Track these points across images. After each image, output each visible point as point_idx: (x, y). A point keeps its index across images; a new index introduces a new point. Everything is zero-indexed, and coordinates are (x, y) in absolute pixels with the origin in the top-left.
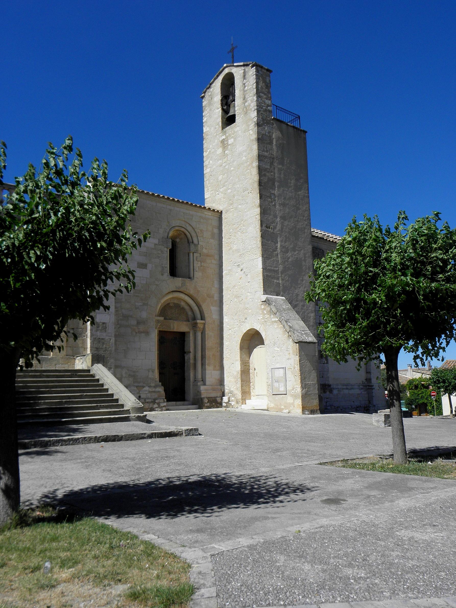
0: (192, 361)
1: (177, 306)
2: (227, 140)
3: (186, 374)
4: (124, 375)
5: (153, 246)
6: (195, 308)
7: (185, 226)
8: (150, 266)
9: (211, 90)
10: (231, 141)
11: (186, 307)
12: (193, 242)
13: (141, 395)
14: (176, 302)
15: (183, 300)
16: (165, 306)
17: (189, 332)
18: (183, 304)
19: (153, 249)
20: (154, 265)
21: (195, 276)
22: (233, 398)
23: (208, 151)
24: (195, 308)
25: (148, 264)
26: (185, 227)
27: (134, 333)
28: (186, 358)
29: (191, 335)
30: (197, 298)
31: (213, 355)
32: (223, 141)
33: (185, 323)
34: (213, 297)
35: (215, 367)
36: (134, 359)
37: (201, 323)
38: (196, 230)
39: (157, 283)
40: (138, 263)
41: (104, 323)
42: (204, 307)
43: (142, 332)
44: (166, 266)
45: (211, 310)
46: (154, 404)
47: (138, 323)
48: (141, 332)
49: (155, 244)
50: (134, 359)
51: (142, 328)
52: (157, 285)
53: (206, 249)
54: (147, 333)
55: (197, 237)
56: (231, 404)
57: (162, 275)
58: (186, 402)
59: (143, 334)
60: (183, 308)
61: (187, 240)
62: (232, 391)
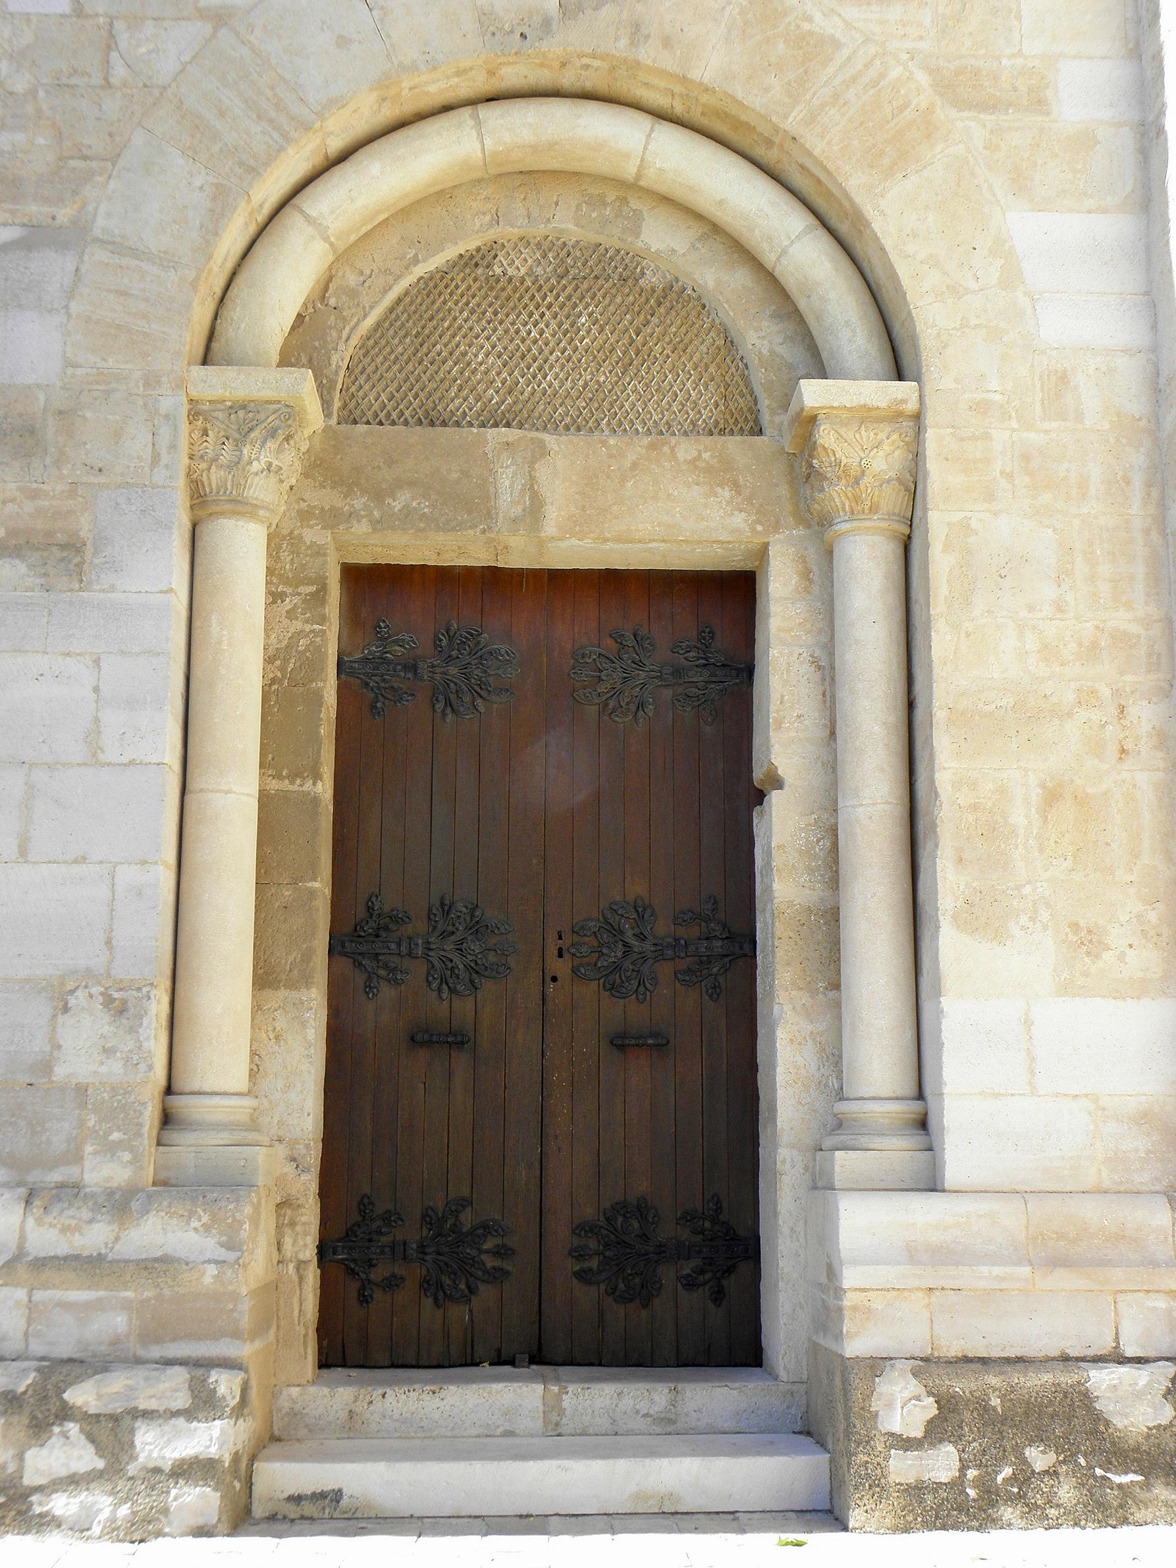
1: (599, 278)
6: (808, 259)
11: (717, 280)
15: (667, 201)
18: (661, 240)
24: (808, 259)
30: (791, 123)
31: (1052, 796)
34: (1038, 102)
35: (1087, 940)
37: (865, 416)
42: (897, 221)
46: (39, 1429)
54: (61, 554)
58: (712, 1396)
60: (675, 297)
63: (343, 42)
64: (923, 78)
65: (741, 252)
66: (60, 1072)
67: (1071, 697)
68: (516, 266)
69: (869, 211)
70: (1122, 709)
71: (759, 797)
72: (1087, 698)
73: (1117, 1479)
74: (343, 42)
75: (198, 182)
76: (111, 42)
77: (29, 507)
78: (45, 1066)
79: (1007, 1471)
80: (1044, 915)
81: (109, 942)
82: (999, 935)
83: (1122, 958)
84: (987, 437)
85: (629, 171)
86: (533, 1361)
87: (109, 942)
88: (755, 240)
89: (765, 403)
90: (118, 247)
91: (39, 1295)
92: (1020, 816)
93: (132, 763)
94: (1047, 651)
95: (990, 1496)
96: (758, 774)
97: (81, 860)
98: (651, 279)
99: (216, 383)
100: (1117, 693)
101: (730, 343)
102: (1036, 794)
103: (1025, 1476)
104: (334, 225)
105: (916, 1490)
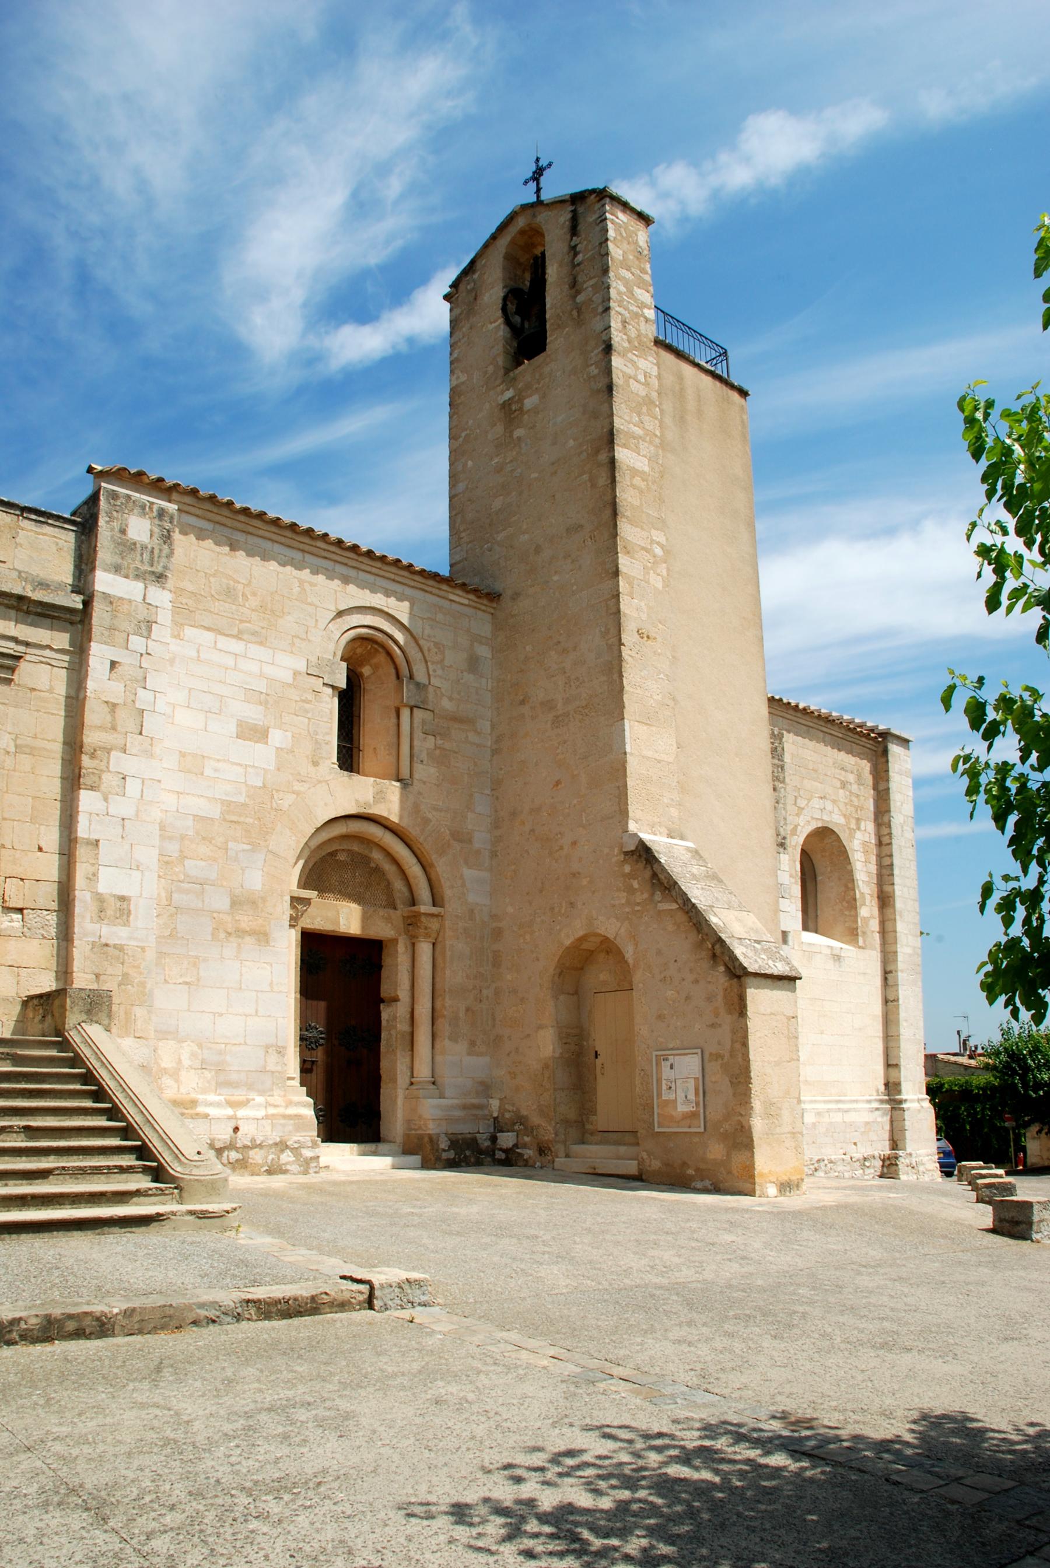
0: (403, 1027)
1: (363, 861)
2: (521, 401)
3: (384, 1064)
4: (186, 1062)
8: (277, 737)
9: (476, 276)
10: (529, 403)
11: (388, 867)
12: (411, 677)
14: (356, 847)
16: (323, 860)
17: (394, 941)
18: (376, 855)
19: (289, 685)
20: (289, 734)
21: (416, 776)
22: (527, 1139)
23: (463, 435)
25: (270, 730)
27: (222, 935)
28: (384, 1016)
29: (402, 947)
30: (421, 840)
31: (468, 1010)
32: (506, 406)
33: (382, 912)
35: (473, 1043)
36: (221, 1015)
39: (297, 787)
40: (240, 724)
41: (123, 899)
42: (442, 867)
44: (327, 738)
45: (462, 877)
46: (282, 1151)
47: (236, 903)
48: (241, 933)
49: (296, 674)
50: (221, 1015)
54: (262, 937)
56: (521, 1155)
58: (382, 1147)
59: (249, 940)
60: (378, 870)
61: (393, 671)
62: (526, 1118)
65: (395, 861)
68: (342, 857)
72: (475, 987)
74: (326, 804)
76: (273, 797)
82: (456, 1042)
85: (376, 840)
88: (401, 862)
92: (462, 1015)
94: (468, 977)
95: (461, 1161)
98: (373, 865)
101: (389, 884)
105: (448, 1160)
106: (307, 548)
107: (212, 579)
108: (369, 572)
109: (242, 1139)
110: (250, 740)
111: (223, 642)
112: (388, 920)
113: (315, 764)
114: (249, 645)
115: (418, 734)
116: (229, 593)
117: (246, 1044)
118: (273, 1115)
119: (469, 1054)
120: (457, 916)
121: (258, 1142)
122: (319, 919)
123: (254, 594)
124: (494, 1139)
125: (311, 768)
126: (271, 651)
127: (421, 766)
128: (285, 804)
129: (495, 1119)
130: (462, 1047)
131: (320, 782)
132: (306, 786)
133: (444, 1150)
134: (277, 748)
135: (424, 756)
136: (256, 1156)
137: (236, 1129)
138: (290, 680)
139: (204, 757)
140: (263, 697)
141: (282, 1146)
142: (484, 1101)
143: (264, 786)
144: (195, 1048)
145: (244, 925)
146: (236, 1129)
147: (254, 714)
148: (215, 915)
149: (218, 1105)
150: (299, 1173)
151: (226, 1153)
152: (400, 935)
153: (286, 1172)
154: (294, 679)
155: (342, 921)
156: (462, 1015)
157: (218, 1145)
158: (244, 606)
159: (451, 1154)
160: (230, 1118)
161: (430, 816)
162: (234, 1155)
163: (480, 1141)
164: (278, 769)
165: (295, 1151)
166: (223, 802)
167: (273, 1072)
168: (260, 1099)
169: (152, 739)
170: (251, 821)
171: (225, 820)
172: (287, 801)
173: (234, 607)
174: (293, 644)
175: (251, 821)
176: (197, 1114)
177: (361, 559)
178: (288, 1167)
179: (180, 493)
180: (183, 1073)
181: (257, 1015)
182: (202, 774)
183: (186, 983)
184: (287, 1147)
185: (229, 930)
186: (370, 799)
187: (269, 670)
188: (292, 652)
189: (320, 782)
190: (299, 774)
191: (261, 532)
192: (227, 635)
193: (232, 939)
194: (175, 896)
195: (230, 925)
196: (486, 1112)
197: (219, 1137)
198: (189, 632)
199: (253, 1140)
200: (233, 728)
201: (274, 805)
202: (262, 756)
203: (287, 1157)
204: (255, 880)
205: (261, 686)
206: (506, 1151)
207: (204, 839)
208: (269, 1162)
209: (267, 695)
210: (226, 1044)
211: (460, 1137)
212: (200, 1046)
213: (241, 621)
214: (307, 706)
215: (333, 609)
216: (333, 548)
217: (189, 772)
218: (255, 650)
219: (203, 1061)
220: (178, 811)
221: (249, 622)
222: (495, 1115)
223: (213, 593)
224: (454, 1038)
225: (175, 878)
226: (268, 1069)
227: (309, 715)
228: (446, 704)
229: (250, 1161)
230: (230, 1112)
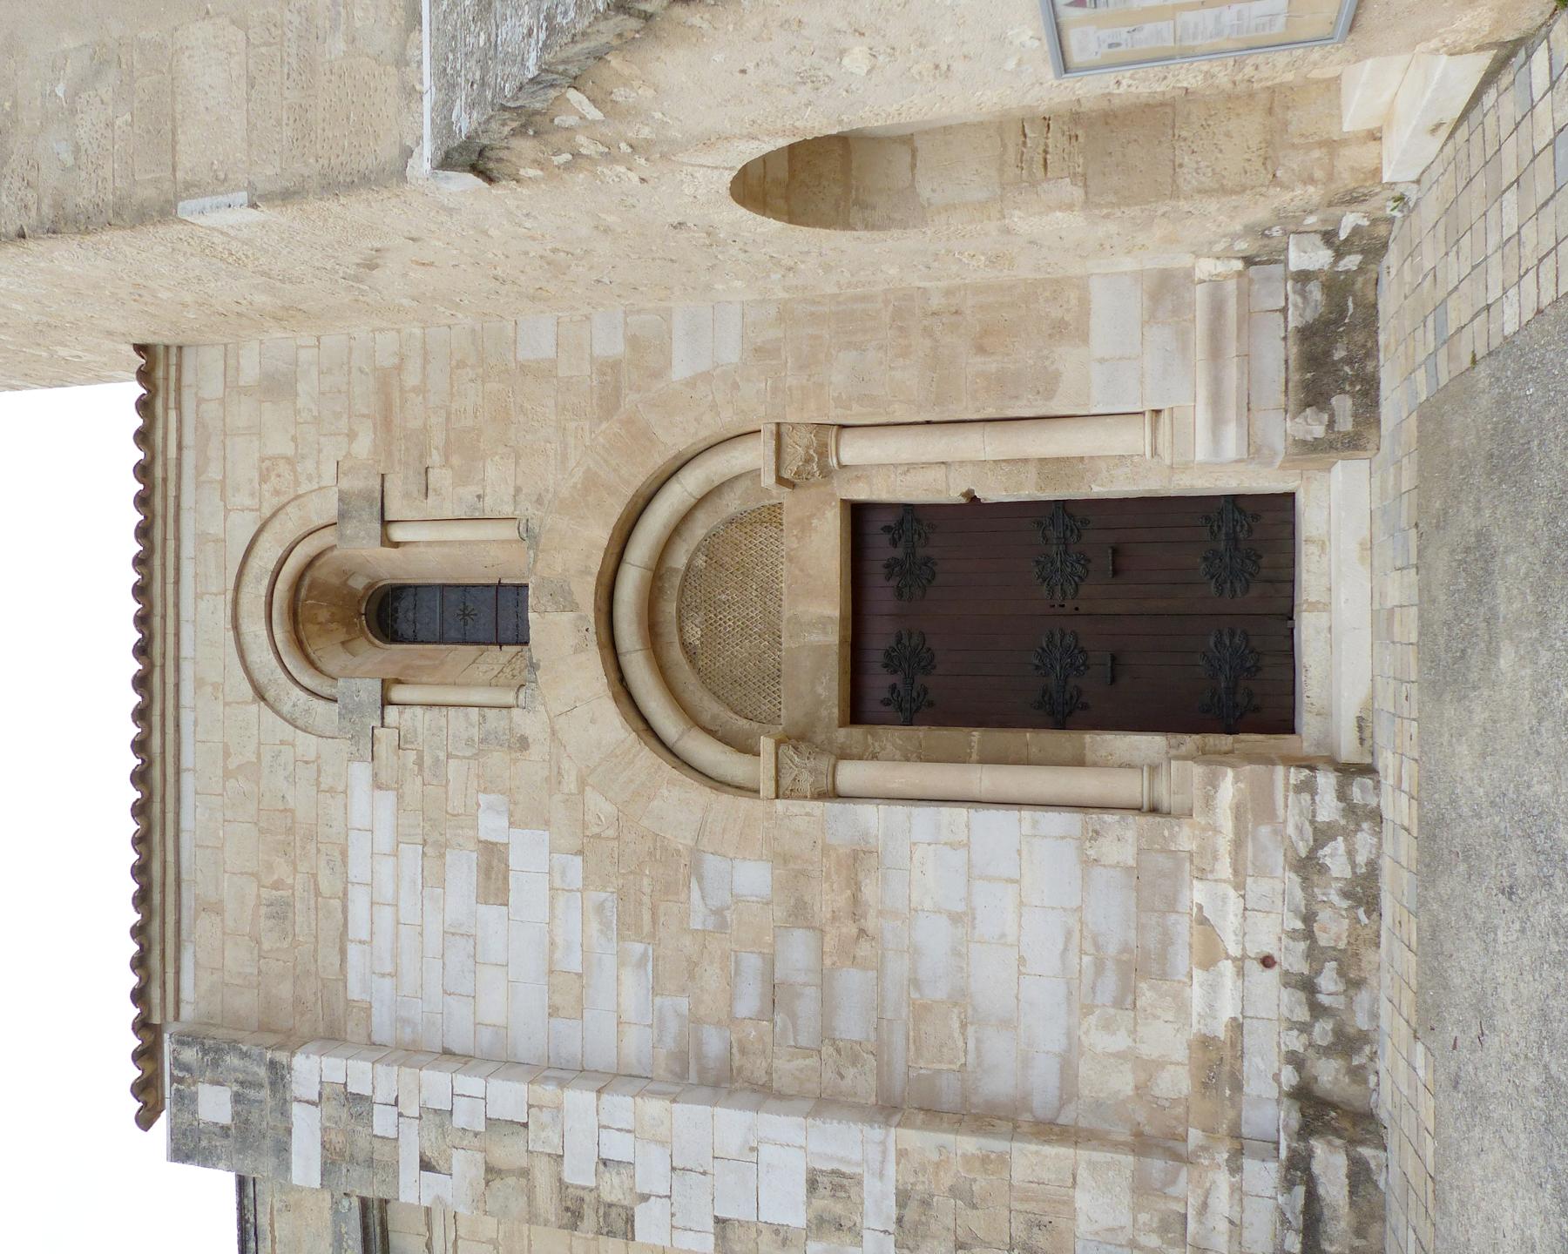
4: (1120, 1042)
5: (387, 799)
7: (259, 581)
8: (492, 826)
13: (1256, 949)
19: (400, 798)
21: (507, 510)
25: (482, 838)
26: (266, 582)
27: (864, 949)
29: (861, 493)
31: (981, 350)
33: (790, 542)
34: (615, 366)
36: (1022, 960)
38: (267, 513)
39: (570, 785)
41: (812, 1184)
43: (855, 899)
45: (691, 383)
46: (1323, 869)
48: (856, 908)
49: (377, 785)
50: (1022, 960)
51: (827, 899)
52: (582, 783)
53: (352, 436)
55: (297, 497)
57: (524, 743)
59: (869, 891)
63: (593, 721)
64: (604, 425)
66: (1132, 862)
67: (928, 343)
69: (673, 453)
70: (934, 314)
71: (973, 499)
72: (928, 332)
73: (1351, 311)
74: (593, 721)
75: (666, 793)
76: (598, 836)
77: (835, 877)
78: (1128, 869)
79: (1347, 369)
80: (1045, 352)
81: (1063, 838)
82: (1056, 377)
83: (1068, 310)
84: (790, 389)
85: (650, 574)
86: (1291, 618)
87: (1063, 838)
89: (767, 502)
90: (700, 832)
91: (1250, 872)
92: (992, 365)
93: (967, 826)
96: (964, 501)
97: (1019, 852)
99: (767, 787)
100: (926, 315)
102: (979, 359)
103: (1349, 361)
104: (682, 726)
106: (170, 770)
107: (266, 946)
108: (177, 635)
109: (1294, 959)
110: (506, 878)
111: (359, 926)
112: (804, 525)
113: (524, 743)
114: (351, 878)
115: (432, 507)
116: (280, 912)
117: (1079, 909)
118: (1236, 872)
119: (1084, 337)
120: (775, 390)
121: (1299, 925)
122: (820, 690)
123: (270, 867)
124: (1303, 277)
125: (536, 752)
126: (353, 834)
127: (489, 501)
128: (608, 809)
129: (1249, 261)
130: (1067, 358)
131: (553, 733)
132: (566, 764)
133: (1331, 424)
134: (511, 824)
135: (468, 492)
136: (1333, 929)
137: (1267, 962)
138: (390, 797)
139: (551, 972)
140: (429, 850)
141: (1308, 867)
142: (1200, 294)
143: (580, 852)
144: (1092, 1019)
145: (842, 900)
146: (1267, 962)
147: (463, 870)
148: (828, 962)
149: (1213, 988)
150: (1378, 834)
151: (1323, 999)
152: (833, 495)
153: (1373, 868)
154: (388, 788)
155: (816, 638)
156: (992, 365)
157: (1303, 1014)
158: (292, 887)
159: (1343, 404)
160: (1241, 973)
161: (579, 475)
162: (1328, 982)
163: (1310, 316)
164: (547, 823)
165: (1323, 834)
166: (621, 937)
167: (1140, 851)
168: (1198, 893)
169: (530, 1106)
170: (646, 881)
171: (653, 935)
172: (599, 806)
173: (298, 905)
174: (331, 790)
175: (646, 881)
176: (1233, 1045)
177: (158, 661)
178: (1361, 859)
179: (150, 1011)
180: (1146, 1051)
181: (1017, 882)
182: (580, 976)
183: (963, 1026)
184: (1312, 855)
185: (855, 931)
186: (567, 617)
187: (384, 840)
188: (345, 792)
189: (553, 733)
190: (547, 779)
191: (170, 858)
192: (346, 919)
193: (871, 924)
194: (803, 1040)
195: (844, 930)
196: (1231, 286)
197: (1285, 1012)
198: (355, 992)
199: (1293, 935)
200: (491, 913)
201: (611, 833)
202: (529, 854)
203: (1335, 858)
204: (753, 877)
205: (411, 853)
206: (1339, 255)
207: (692, 977)
208: (1345, 904)
209: (425, 843)
210: (1082, 952)
211: (1295, 377)
212: (1088, 1010)
213: (318, 893)
214: (428, 761)
215: (254, 708)
216: (156, 720)
217: (580, 1000)
218: (358, 868)
219: (1118, 1003)
220: (651, 1026)
221: (315, 876)
222: (1238, 265)
223: (285, 945)
224: (1049, 383)
225: (768, 1039)
226: (1132, 862)
227: (442, 756)
228: (363, 446)
229: (1342, 945)
230: (1227, 967)
